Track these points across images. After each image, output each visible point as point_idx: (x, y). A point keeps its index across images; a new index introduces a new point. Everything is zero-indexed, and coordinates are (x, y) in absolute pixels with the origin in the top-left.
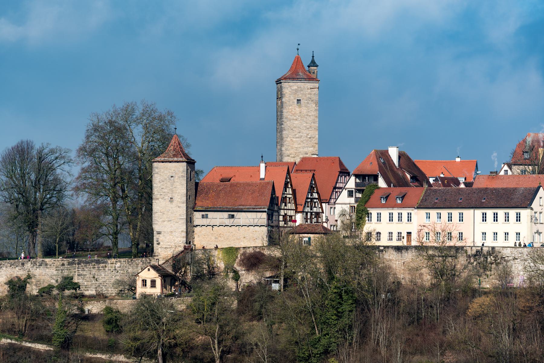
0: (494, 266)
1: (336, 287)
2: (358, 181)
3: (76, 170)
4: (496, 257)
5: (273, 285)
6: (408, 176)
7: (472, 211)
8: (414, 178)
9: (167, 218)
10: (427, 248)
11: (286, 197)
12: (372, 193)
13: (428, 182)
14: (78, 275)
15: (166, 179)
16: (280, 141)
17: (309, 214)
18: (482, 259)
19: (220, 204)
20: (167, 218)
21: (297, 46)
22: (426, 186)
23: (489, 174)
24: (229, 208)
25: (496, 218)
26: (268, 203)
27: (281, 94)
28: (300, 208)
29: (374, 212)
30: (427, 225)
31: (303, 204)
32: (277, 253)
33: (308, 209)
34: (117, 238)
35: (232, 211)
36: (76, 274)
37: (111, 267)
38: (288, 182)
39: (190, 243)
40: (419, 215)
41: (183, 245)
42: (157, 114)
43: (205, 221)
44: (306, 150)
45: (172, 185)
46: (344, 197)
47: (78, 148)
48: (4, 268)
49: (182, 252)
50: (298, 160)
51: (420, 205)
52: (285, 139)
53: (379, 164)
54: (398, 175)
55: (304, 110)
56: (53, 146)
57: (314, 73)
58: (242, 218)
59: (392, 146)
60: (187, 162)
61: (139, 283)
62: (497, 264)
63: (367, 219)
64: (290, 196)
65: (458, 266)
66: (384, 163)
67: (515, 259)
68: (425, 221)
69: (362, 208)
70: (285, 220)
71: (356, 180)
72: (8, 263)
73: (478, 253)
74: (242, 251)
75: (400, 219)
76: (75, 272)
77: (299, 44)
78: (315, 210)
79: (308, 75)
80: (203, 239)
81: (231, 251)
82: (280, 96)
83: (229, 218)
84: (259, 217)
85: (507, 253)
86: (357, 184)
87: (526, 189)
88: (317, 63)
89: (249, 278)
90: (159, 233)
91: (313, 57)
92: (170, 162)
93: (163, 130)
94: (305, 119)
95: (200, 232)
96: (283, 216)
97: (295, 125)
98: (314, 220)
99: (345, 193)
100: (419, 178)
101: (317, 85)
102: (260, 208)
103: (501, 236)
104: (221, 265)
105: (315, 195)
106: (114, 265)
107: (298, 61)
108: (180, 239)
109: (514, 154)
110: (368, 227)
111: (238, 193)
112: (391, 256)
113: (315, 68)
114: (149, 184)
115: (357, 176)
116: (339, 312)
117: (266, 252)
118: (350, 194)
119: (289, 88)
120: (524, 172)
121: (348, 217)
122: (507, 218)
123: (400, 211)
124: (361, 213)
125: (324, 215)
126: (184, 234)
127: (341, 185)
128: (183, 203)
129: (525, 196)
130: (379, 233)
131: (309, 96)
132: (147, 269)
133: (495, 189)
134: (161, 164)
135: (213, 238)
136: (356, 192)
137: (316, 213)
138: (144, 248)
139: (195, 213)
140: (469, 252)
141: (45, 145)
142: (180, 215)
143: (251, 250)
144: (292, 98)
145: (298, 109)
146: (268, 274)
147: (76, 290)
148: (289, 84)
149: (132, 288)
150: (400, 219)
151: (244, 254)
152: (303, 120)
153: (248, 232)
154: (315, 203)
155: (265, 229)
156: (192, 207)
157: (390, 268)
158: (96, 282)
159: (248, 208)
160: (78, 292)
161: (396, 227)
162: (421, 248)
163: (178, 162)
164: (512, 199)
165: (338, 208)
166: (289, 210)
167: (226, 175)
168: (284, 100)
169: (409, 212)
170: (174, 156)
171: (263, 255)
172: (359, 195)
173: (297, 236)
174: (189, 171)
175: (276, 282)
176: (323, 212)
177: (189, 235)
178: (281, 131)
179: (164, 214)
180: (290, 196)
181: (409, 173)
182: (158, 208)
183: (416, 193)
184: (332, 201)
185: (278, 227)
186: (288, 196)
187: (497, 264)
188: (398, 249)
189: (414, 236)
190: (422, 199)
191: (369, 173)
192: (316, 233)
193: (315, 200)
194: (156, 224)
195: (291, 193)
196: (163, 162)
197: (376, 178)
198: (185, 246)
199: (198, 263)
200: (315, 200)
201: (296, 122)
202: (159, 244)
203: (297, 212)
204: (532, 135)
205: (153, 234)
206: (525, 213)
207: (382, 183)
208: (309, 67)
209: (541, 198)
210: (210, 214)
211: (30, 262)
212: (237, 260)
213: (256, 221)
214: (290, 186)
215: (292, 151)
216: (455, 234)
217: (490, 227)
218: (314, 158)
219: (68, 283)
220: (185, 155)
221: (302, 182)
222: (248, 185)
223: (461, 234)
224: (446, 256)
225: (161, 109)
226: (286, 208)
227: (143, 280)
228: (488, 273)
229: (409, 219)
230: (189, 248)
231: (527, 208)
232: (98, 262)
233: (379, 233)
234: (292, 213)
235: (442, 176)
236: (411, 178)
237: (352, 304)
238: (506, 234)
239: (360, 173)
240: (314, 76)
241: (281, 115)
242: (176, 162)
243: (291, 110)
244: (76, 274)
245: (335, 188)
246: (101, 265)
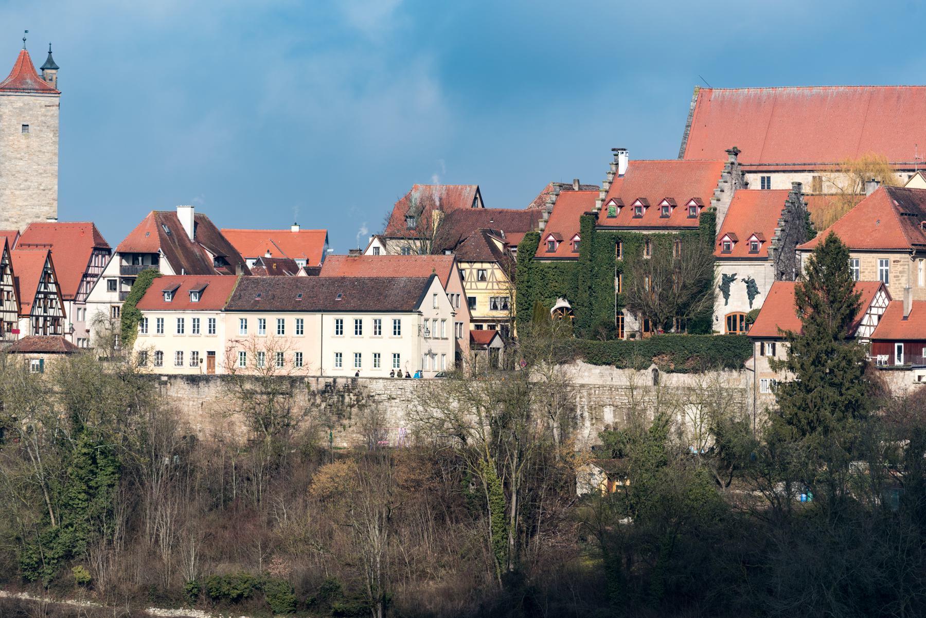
0: (355, 410)
1: (85, 444)
2: (124, 263)
6: (211, 257)
7: (318, 316)
8: (220, 259)
10: (241, 379)
11: (2, 290)
12: (148, 284)
13: (244, 267)
17: (41, 320)
18: (335, 398)
21: (24, 35)
22: (240, 273)
23: (348, 254)
25: (358, 329)
28: (26, 310)
29: (152, 317)
31: (32, 302)
33: (39, 311)
38: (6, 265)
40: (228, 323)
44: (36, 210)
46: (100, 292)
50: (23, 228)
51: (230, 306)
53: (160, 235)
54: (192, 253)
55: (34, 143)
57: (51, 80)
59: (184, 204)
62: (361, 407)
63: (139, 328)
64: (10, 288)
65: (295, 411)
67: (391, 398)
68: (238, 333)
69: (131, 309)
71: (121, 262)
73: (330, 388)
75: (196, 329)
77: (26, 32)
78: (51, 312)
85: (377, 387)
86: (123, 270)
87: (410, 280)
88: (57, 62)
91: (50, 53)
94: (35, 159)
97: (18, 168)
98: (50, 330)
99: (103, 284)
100: (228, 259)
101: (56, 100)
103: (367, 360)
105: (52, 288)
107: (24, 60)
109: (391, 219)
110: (142, 342)
112: (180, 393)
113: (54, 71)
115: (123, 255)
116: (90, 487)
118: (112, 285)
120: (406, 250)
121: (107, 325)
122: (378, 330)
123: (196, 316)
124: (130, 318)
125: (67, 321)
129: (409, 292)
131: (43, 118)
133: (358, 280)
136: (121, 283)
137: (53, 317)
140: (314, 387)
144: (14, 121)
145: (23, 141)
148: (10, 98)
150: (196, 329)
154: (52, 300)
157: (178, 412)
161: (190, 343)
162: (231, 379)
164: (386, 296)
165: (92, 310)
166: (6, 311)
169: (212, 316)
172: (127, 288)
173: (20, 357)
176: (65, 317)
180: (10, 288)
181: (213, 250)
183: (224, 284)
184: (81, 298)
186: (6, 288)
187: (361, 407)
188: (193, 380)
189: (220, 358)
190: (235, 296)
192: (53, 352)
193: (52, 296)
195: (11, 283)
197: (155, 258)
201: (21, 163)
203: (20, 315)
204: (421, 187)
206: (408, 321)
207: (165, 267)
208: (43, 69)
209: (435, 295)
214: (8, 272)
215: (13, 212)
216: (290, 355)
217: (349, 343)
218: (51, 224)
223: (299, 355)
224: (274, 393)
228: (346, 422)
229: (212, 329)
231: (411, 311)
233: (159, 353)
234: (12, 317)
235: (268, 256)
236: (216, 259)
237: (113, 473)
238: (377, 356)
239: (128, 251)
240: (51, 85)
245: (86, 275)
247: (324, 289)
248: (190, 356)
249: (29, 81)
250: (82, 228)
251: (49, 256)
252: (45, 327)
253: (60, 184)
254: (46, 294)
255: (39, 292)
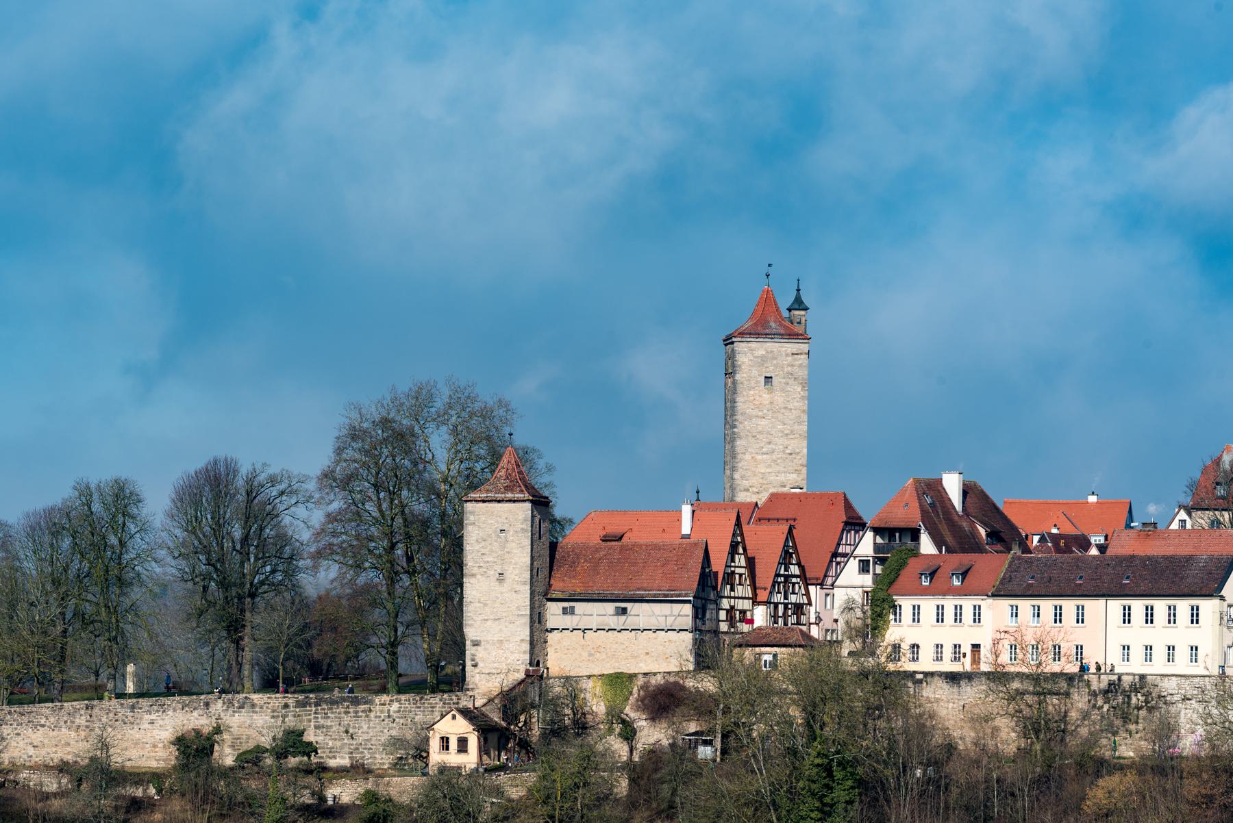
0: (1143, 713)
1: (819, 754)
2: (879, 540)
3: (317, 517)
4: (1147, 695)
5: (701, 749)
6: (982, 532)
8: (994, 535)
9: (492, 613)
11: (733, 572)
12: (902, 565)
14: (316, 727)
15: (490, 536)
16: (729, 459)
17: (781, 607)
18: (1120, 699)
19: (600, 584)
20: (492, 613)
21: (766, 269)
22: (1016, 550)
24: (618, 595)
25: (1149, 617)
26: (696, 585)
27: (734, 366)
28: (763, 595)
30: (1011, 630)
32: (708, 684)
33: (778, 598)
34: (394, 654)
35: (623, 599)
36: (312, 724)
37: (382, 712)
39: (538, 664)
40: (996, 611)
41: (523, 669)
42: (477, 406)
43: (568, 621)
44: (782, 478)
45: (503, 547)
47: (319, 473)
48: (170, 713)
49: (523, 681)
50: (762, 499)
51: (998, 590)
52: (739, 456)
53: (921, 506)
54: (961, 529)
55: (779, 398)
56: (274, 470)
58: (642, 613)
59: (950, 470)
60: (532, 501)
61: (435, 744)
62: (1151, 710)
63: (892, 617)
65: (1073, 715)
66: (933, 505)
67: (1185, 699)
68: (1010, 623)
69: (881, 595)
70: (731, 619)
72: (178, 702)
73: (1113, 688)
74: (640, 681)
75: (958, 618)
76: (310, 721)
78: (793, 599)
79: (786, 328)
80: (562, 658)
81: (618, 682)
82: (730, 372)
83: (617, 614)
84: (676, 612)
85: (1169, 686)
86: (877, 548)
87: (1211, 558)
89: (652, 735)
90: (476, 644)
91: (798, 290)
92: (499, 501)
93: (489, 438)
94: (781, 417)
95: (559, 642)
96: (728, 611)
97: (760, 428)
98: (792, 619)
99: (853, 565)
100: (1004, 534)
101: (805, 347)
102: (679, 595)
103: (1160, 653)
104: (598, 707)
105: (794, 570)
106: (386, 708)
107: (768, 300)
108: (517, 656)
109: (1194, 487)
110: (894, 633)
111: (635, 564)
112: (936, 692)
113: (802, 313)
114: (457, 545)
115: (877, 531)
116: (825, 805)
117: (690, 683)
118: (864, 567)
119: (749, 353)
120: (1216, 523)
121: (859, 614)
123: (958, 603)
124: (880, 606)
125: (812, 609)
126: (527, 647)
127: (848, 549)
128: (525, 584)
130: (915, 647)
132: (450, 716)
133: (1149, 558)
134: (481, 504)
135: (585, 654)
136: (875, 563)
137: (795, 604)
138: (445, 675)
139: (549, 604)
140: (1095, 686)
141: (258, 467)
142: (518, 608)
143: (659, 680)
144: (755, 373)
145: (766, 396)
146: (693, 727)
147: (309, 757)
149: (421, 753)
150: (958, 618)
151: (645, 687)
152: (776, 418)
153: (655, 641)
154: (794, 584)
155: (688, 637)
156: (541, 594)
157: (932, 716)
158: (351, 741)
159: (655, 595)
160: (314, 760)
161: (949, 635)
162: (998, 677)
163: (514, 501)
164: (1182, 578)
165: (840, 596)
167: (613, 529)
168: (738, 377)
170: (507, 489)
171: (683, 688)
172: (879, 569)
173: (748, 653)
174: (537, 520)
175: (706, 743)
176: (810, 604)
177: (537, 650)
178: (733, 441)
179: (485, 605)
180: (742, 571)
181: (984, 524)
182: (474, 593)
183: (993, 564)
184: (829, 581)
185: (716, 632)
186: (738, 570)
187: (1151, 710)
190: (1004, 578)
191: (902, 525)
192: (790, 646)
193: (794, 580)
194: (471, 625)
195: (743, 564)
196: (484, 501)
197: (915, 535)
198: (527, 671)
199: (553, 705)
200: (794, 580)
201: (764, 422)
202: (475, 666)
203: (756, 602)
205: (464, 645)
206: (1208, 607)
207: (927, 546)
208: (790, 310)
210: (580, 607)
211: (220, 701)
212: (632, 699)
213: (670, 620)
214: (741, 551)
215: (754, 481)
216: (1067, 648)
217: (1138, 634)
219: (293, 743)
220: (529, 488)
221: (766, 542)
222: (656, 547)
223: (1079, 648)
225: (486, 395)
226: (732, 594)
227: (442, 738)
228: (1132, 727)
229: (977, 619)
230: (535, 675)
232: (356, 702)
233: (915, 647)
234: (746, 605)
235: (1054, 531)
236: (988, 535)
237: (852, 788)
238: (1171, 649)
239: (883, 526)
240: (799, 329)
241: (733, 408)
242: (510, 501)
243: (752, 398)
244: (312, 724)
245: (835, 554)
246: (362, 707)
247: (1110, 570)
248: (951, 649)
249: (773, 324)
250: (830, 499)
251: (790, 532)
252: (785, 616)
253: (810, 447)
254: (787, 577)
255: (778, 575)
